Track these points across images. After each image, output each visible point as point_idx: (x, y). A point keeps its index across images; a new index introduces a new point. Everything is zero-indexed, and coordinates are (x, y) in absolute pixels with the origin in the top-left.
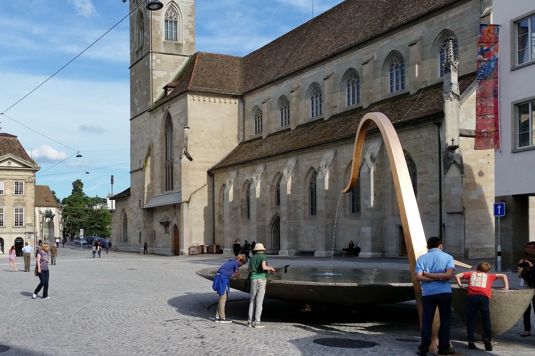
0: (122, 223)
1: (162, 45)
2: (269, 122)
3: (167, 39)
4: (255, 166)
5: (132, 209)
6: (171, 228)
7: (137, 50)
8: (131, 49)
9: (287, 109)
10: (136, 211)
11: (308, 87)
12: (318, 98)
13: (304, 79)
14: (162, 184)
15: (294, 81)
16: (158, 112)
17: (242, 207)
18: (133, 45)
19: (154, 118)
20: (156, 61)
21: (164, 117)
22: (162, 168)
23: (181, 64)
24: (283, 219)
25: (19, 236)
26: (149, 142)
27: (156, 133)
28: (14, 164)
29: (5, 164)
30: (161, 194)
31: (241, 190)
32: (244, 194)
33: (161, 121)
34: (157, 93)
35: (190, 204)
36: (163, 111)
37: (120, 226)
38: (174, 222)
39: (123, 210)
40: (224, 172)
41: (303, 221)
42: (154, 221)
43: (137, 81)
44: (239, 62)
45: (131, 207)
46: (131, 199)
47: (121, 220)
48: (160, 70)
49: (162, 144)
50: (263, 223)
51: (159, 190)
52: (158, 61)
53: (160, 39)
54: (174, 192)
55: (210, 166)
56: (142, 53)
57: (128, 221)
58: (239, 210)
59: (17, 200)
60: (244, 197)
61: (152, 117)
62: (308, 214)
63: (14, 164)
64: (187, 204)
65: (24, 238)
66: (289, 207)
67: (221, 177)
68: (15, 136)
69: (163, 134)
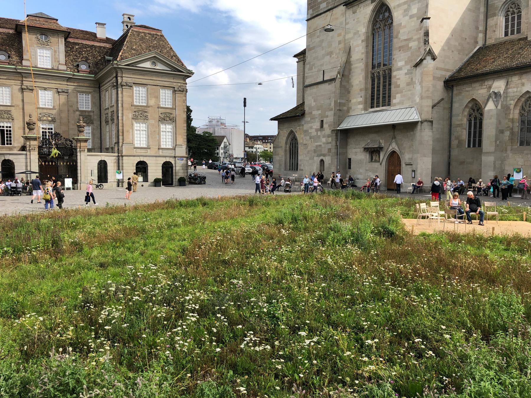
0: (288, 148)
5: (306, 131)
14: (366, 99)
21: (373, 11)
25: (168, 159)
26: (342, 46)
27: (357, 33)
28: (160, 67)
29: (147, 65)
37: (286, 151)
42: (349, 147)
45: (305, 128)
46: (307, 118)
47: (286, 143)
51: (361, 106)
54: (392, 108)
57: (299, 146)
59: (165, 113)
61: (350, 12)
63: (160, 67)
65: (173, 162)
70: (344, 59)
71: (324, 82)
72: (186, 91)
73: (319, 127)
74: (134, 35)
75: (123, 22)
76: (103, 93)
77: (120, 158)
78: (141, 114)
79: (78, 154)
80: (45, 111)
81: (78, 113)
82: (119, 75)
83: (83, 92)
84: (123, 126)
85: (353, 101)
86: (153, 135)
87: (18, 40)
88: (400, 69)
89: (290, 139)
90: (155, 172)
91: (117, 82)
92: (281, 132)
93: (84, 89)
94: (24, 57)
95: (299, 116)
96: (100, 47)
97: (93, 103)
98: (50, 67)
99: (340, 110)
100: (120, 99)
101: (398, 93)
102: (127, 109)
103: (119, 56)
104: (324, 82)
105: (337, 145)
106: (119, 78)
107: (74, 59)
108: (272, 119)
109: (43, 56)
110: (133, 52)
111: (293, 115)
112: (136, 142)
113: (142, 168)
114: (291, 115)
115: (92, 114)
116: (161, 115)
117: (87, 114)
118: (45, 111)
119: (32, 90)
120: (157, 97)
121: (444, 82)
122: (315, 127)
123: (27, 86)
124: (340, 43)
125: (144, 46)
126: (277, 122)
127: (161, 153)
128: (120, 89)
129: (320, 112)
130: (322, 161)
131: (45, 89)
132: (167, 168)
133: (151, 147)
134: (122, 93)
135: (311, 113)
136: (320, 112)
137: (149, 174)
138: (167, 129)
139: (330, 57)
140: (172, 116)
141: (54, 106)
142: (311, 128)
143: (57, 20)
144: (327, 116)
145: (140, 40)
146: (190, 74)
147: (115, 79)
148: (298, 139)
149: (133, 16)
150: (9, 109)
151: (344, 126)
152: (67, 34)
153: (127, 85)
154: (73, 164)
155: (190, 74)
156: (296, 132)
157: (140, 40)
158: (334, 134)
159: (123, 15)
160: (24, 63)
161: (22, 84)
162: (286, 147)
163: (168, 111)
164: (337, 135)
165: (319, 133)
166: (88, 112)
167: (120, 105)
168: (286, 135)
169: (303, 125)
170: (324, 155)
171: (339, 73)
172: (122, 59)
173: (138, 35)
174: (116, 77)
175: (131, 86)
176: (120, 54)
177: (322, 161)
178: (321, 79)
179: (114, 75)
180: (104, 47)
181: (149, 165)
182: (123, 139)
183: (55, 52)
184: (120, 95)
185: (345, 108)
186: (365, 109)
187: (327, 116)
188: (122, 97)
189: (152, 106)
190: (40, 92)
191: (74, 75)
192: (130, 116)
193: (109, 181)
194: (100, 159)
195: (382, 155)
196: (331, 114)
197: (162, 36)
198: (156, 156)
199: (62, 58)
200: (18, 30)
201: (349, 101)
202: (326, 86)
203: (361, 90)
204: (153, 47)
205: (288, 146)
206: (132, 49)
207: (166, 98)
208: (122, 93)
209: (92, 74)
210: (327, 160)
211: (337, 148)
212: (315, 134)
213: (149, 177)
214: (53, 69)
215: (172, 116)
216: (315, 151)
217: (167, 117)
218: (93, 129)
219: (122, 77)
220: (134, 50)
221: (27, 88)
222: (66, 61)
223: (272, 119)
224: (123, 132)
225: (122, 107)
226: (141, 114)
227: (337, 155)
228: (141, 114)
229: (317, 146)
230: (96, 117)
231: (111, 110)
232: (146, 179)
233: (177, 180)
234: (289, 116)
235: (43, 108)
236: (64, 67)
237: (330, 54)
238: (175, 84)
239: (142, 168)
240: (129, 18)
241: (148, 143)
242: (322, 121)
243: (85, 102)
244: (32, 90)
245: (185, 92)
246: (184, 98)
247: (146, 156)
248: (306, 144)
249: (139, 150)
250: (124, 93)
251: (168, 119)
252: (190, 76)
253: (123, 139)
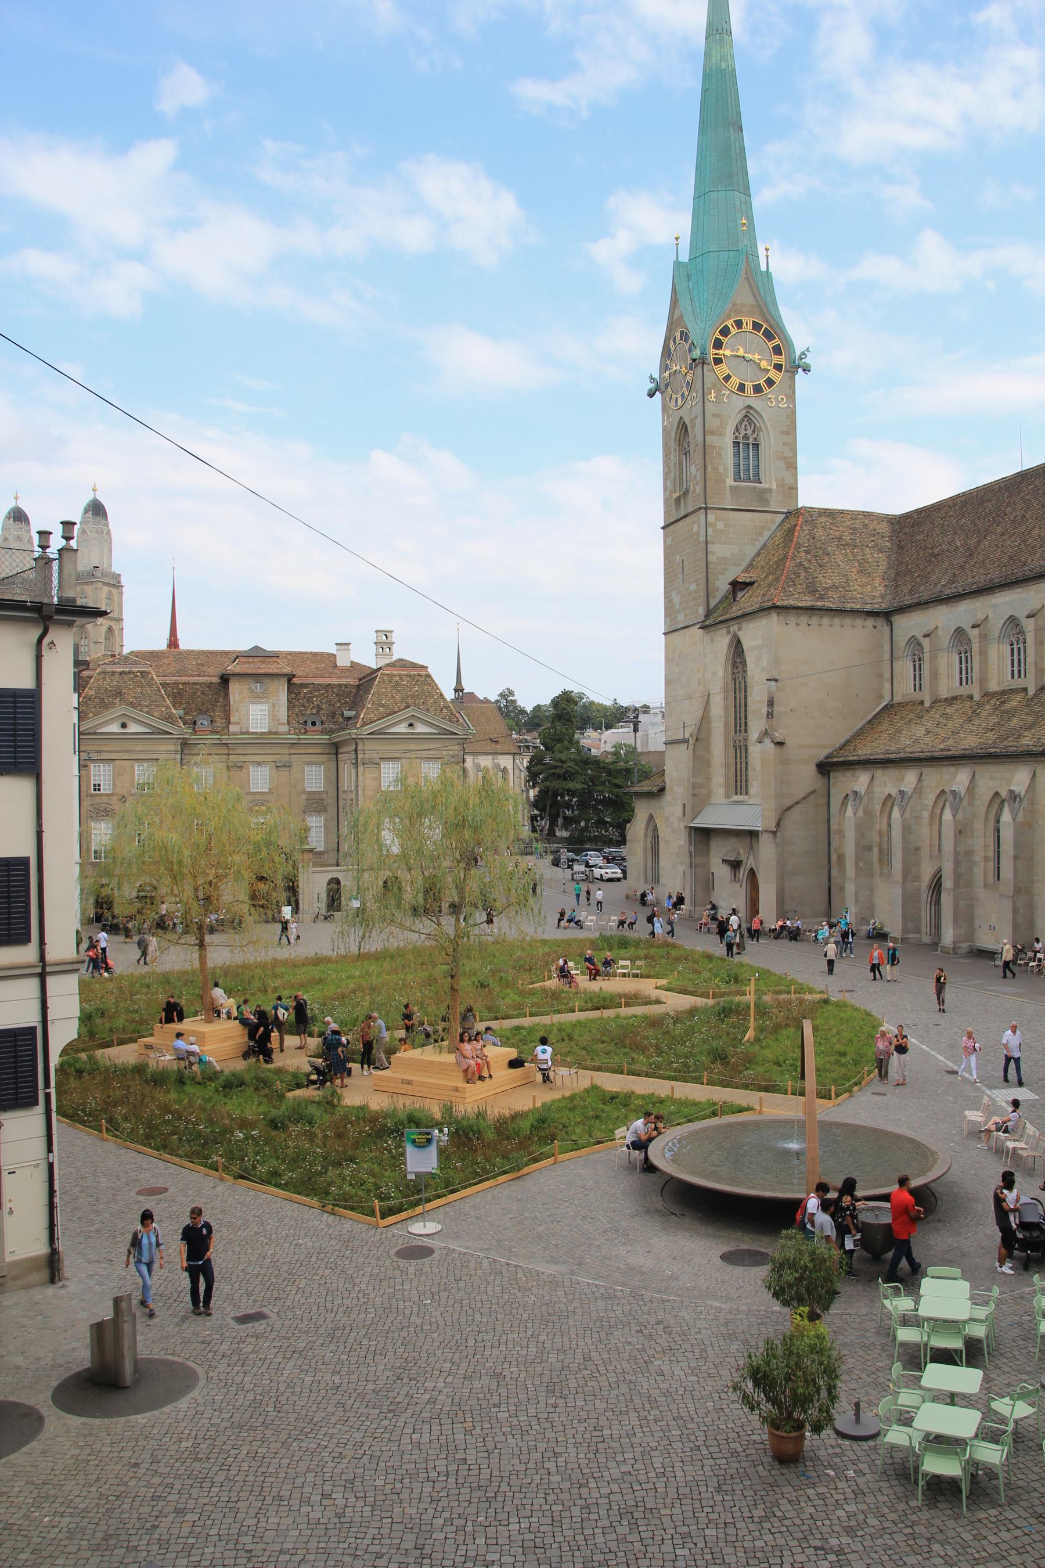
0: (649, 844)
1: (728, 489)
2: (935, 676)
3: (737, 478)
4: (903, 771)
6: (743, 873)
7: (677, 495)
8: (665, 490)
9: (968, 655)
10: (676, 825)
11: (1002, 622)
12: (1021, 646)
13: (995, 606)
15: (978, 604)
16: (718, 633)
17: (880, 845)
18: (669, 483)
19: (712, 641)
20: (714, 525)
22: (726, 745)
23: (769, 529)
24: (948, 884)
29: (402, 728)
31: (878, 812)
32: (885, 820)
33: (724, 652)
34: (717, 590)
35: (778, 834)
36: (728, 632)
37: (645, 848)
38: (749, 863)
39: (651, 817)
40: (848, 770)
41: (982, 889)
43: (678, 560)
44: (884, 528)
47: (646, 836)
48: (724, 543)
49: (725, 698)
50: (915, 884)
52: (720, 525)
53: (724, 482)
55: (821, 754)
56: (686, 505)
58: (876, 850)
60: (885, 827)
62: (991, 878)
64: (771, 835)
66: (957, 863)
67: (842, 779)
68: (422, 667)
69: (730, 678)
70: (699, 714)
74: (384, 681)
76: (341, 764)
80: (258, 797)
81: (304, 796)
82: (360, 747)
83: (312, 763)
91: (357, 759)
96: (340, 686)
97: (327, 779)
100: (360, 783)
107: (300, 711)
109: (258, 713)
110: (382, 709)
115: (324, 796)
117: (317, 796)
118: (258, 797)
128: (361, 769)
131: (259, 764)
145: (394, 688)
151: (701, 822)
157: (394, 688)
160: (233, 728)
162: (646, 842)
164: (690, 836)
173: (390, 682)
180: (346, 686)
183: (274, 706)
184: (360, 778)
194: (330, 876)
197: (429, 676)
199: (283, 713)
205: (649, 840)
209: (326, 734)
214: (270, 733)
218: (326, 821)
220: (383, 706)
230: (331, 801)
235: (255, 793)
236: (286, 728)
243: (314, 777)
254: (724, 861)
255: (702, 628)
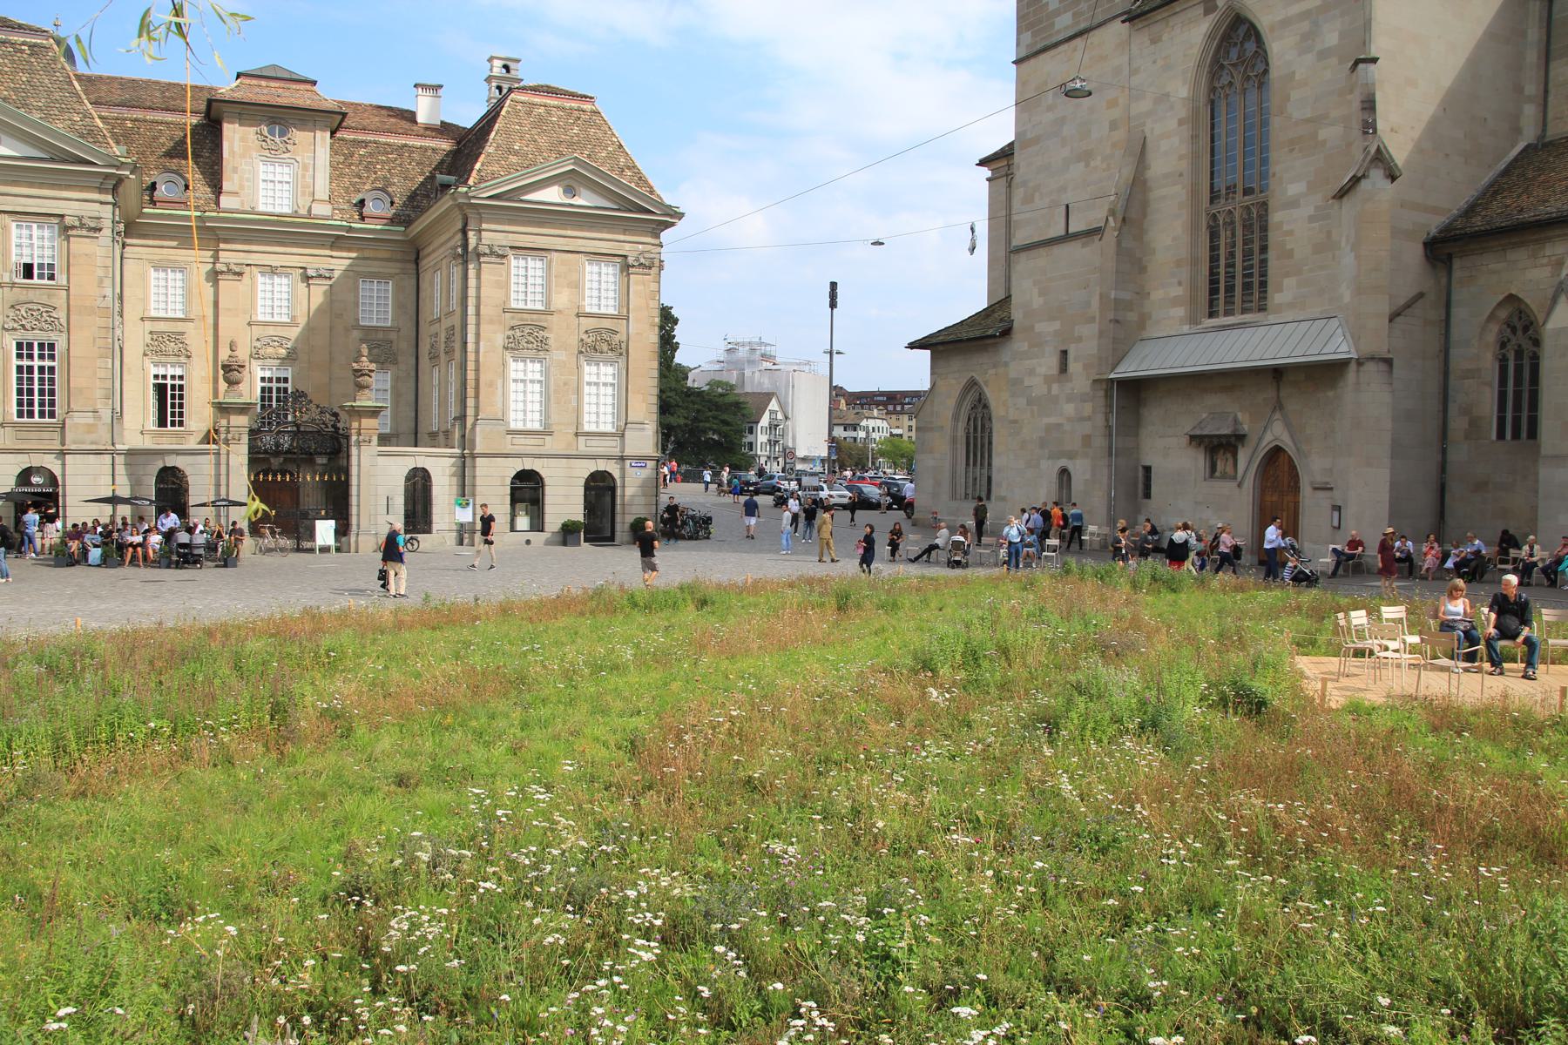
0: (961, 433)
5: (1017, 382)
14: (1193, 287)
21: (1210, 37)
25: (602, 466)
26: (1120, 134)
29: (553, 195)
30: (1186, 329)
37: (954, 440)
45: (1013, 374)
46: (1018, 343)
47: (956, 417)
51: (1180, 312)
54: (1272, 318)
59: (597, 331)
61: (1141, 39)
65: (616, 474)
70: (1128, 172)
71: (1068, 237)
72: (661, 268)
73: (1055, 371)
74: (517, 113)
75: (489, 79)
76: (425, 278)
77: (468, 461)
78: (530, 334)
79: (354, 451)
80: (271, 331)
81: (356, 334)
83: (372, 276)
84: (477, 370)
85: (1157, 295)
86: (562, 395)
87: (212, 142)
88: (1293, 203)
89: (967, 406)
90: (565, 501)
92: (939, 383)
93: (375, 267)
94: (226, 186)
95: (994, 336)
96: (424, 149)
97: (399, 306)
98: (287, 210)
99: (1117, 321)
100: (472, 292)
101: (1287, 275)
102: (491, 322)
103: (474, 173)
104: (1068, 237)
105: (1109, 427)
106: (471, 234)
108: (912, 346)
109: (270, 177)
110: (513, 159)
111: (978, 334)
112: (512, 415)
113: (528, 490)
114: (971, 335)
115: (393, 336)
116: (585, 337)
117: (381, 335)
118: (271, 331)
119: (240, 274)
120: (577, 286)
121: (1425, 244)
122: (1042, 370)
123: (227, 265)
124: (1114, 125)
125: (543, 141)
126: (928, 352)
127: (582, 446)
129: (1057, 325)
130: (1064, 473)
131: (273, 271)
132: (600, 489)
133: (554, 428)
134: (478, 277)
135: (1032, 327)
136: (1057, 325)
137: (548, 509)
138: (600, 377)
139: (1087, 165)
140: (617, 338)
141: (293, 318)
142: (1031, 372)
143: (314, 83)
144: (1080, 339)
145: (535, 125)
146: (672, 216)
147: (459, 236)
148: (993, 404)
149: (518, 61)
150: (180, 327)
151: (1129, 369)
152: (334, 120)
153: (492, 253)
154: (339, 478)
155: (672, 216)
156: (986, 383)
157: (535, 125)
158: (1102, 393)
159: (491, 60)
161: (216, 258)
162: (955, 429)
163: (606, 324)
164: (1108, 396)
165: (1055, 389)
166: (385, 330)
167: (471, 310)
168: (956, 393)
169: (1006, 364)
170: (1071, 456)
171: (1112, 212)
172: (482, 180)
173: (529, 113)
174: (464, 232)
175: (503, 256)
176: (478, 166)
177: (1064, 473)
178: (1059, 230)
179: (459, 225)
181: (547, 481)
182: (477, 408)
184: (472, 282)
185: (1132, 316)
186: (1193, 320)
187: (1080, 339)
188: (478, 288)
189: (560, 312)
190: (260, 279)
191: (350, 229)
192: (500, 339)
193: (435, 527)
194: (410, 463)
195: (1243, 456)
196: (1089, 331)
198: (568, 457)
200: (213, 114)
201: (1142, 294)
202: (1073, 250)
203: (1178, 263)
204: (571, 144)
205: (962, 425)
206: (510, 151)
207: (599, 288)
208: (478, 277)
209: (399, 224)
210: (1080, 470)
211: (1110, 435)
212: (1044, 390)
213: (548, 518)
214: (295, 214)
215: (617, 338)
216: (1043, 443)
217: (602, 343)
218: (396, 380)
219: (480, 231)
220: (516, 153)
221: (229, 271)
222: (332, 191)
223: (912, 346)
224: (477, 388)
225: (478, 314)
226: (529, 335)
227: (1110, 455)
228: (530, 334)
229: (1049, 428)
230: (405, 346)
231: (446, 323)
232: (538, 525)
233: (627, 526)
234: (964, 336)
237: (1086, 157)
238: (628, 246)
239: (528, 490)
240: (506, 67)
241: (547, 417)
242: (1064, 353)
243: (378, 305)
244: (240, 274)
245: (654, 270)
246: (654, 286)
247: (540, 456)
248: (1015, 422)
249: (520, 440)
250: (484, 276)
251: (605, 347)
252: (673, 224)
253: (477, 408)
254: (1192, 438)
255: (1130, 20)
